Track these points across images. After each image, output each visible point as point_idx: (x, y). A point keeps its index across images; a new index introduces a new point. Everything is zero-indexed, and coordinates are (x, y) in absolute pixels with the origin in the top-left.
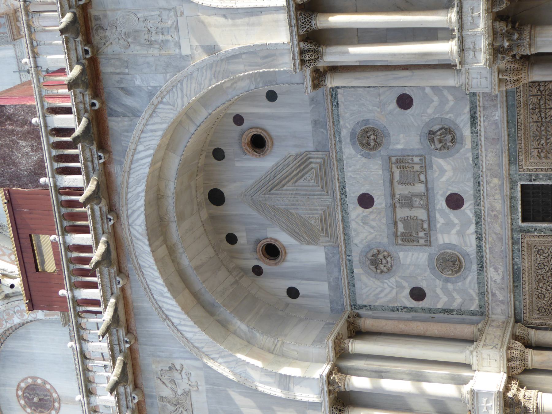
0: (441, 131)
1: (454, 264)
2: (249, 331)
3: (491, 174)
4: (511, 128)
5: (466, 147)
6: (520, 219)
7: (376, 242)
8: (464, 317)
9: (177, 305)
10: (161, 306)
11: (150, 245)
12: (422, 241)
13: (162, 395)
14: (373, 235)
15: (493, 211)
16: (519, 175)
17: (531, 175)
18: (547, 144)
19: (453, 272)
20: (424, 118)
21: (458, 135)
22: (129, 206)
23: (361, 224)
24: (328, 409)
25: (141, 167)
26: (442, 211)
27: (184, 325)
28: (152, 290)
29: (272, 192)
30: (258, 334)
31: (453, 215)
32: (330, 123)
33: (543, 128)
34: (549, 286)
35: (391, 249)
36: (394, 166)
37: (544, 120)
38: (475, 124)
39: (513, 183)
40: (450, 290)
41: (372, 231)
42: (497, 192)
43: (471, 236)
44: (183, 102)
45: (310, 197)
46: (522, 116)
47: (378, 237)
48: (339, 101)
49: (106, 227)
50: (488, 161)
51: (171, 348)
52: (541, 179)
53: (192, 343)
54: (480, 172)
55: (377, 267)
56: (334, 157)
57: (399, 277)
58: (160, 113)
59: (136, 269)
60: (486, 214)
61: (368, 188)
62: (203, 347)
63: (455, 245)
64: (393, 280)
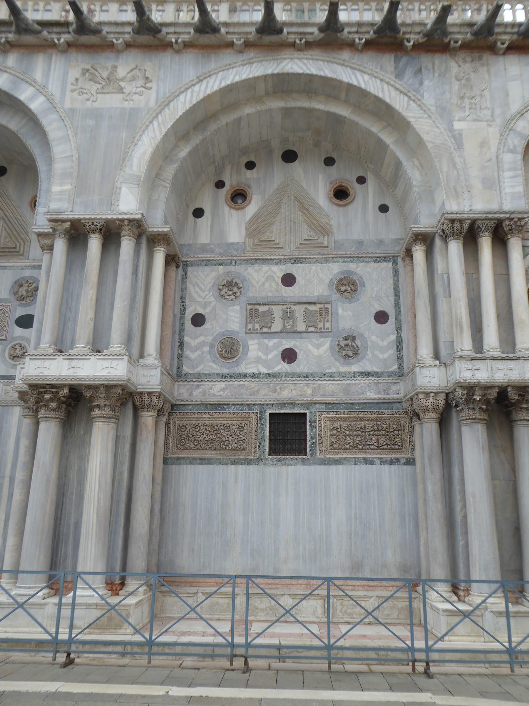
0: (355, 346)
3: (315, 388)
5: (341, 367)
6: (274, 412)
9: (212, 91)
10: (212, 77)
11: (273, 75)
12: (250, 326)
13: (118, 67)
15: (280, 388)
17: (315, 422)
18: (345, 436)
20: (367, 333)
21: (351, 360)
22: (311, 61)
23: (266, 275)
24: (104, 217)
25: (348, 76)
30: (175, 166)
31: (276, 353)
33: (359, 433)
35: (243, 299)
36: (322, 306)
37: (367, 433)
41: (259, 284)
42: (299, 393)
43: (256, 368)
45: (292, 233)
47: (254, 289)
48: (381, 264)
49: (293, 36)
50: (328, 386)
52: (312, 430)
53: (173, 100)
54: (317, 379)
55: (224, 287)
56: (330, 256)
57: (215, 305)
58: (400, 98)
59: (250, 59)
60: (277, 382)
62: (169, 109)
64: (212, 299)
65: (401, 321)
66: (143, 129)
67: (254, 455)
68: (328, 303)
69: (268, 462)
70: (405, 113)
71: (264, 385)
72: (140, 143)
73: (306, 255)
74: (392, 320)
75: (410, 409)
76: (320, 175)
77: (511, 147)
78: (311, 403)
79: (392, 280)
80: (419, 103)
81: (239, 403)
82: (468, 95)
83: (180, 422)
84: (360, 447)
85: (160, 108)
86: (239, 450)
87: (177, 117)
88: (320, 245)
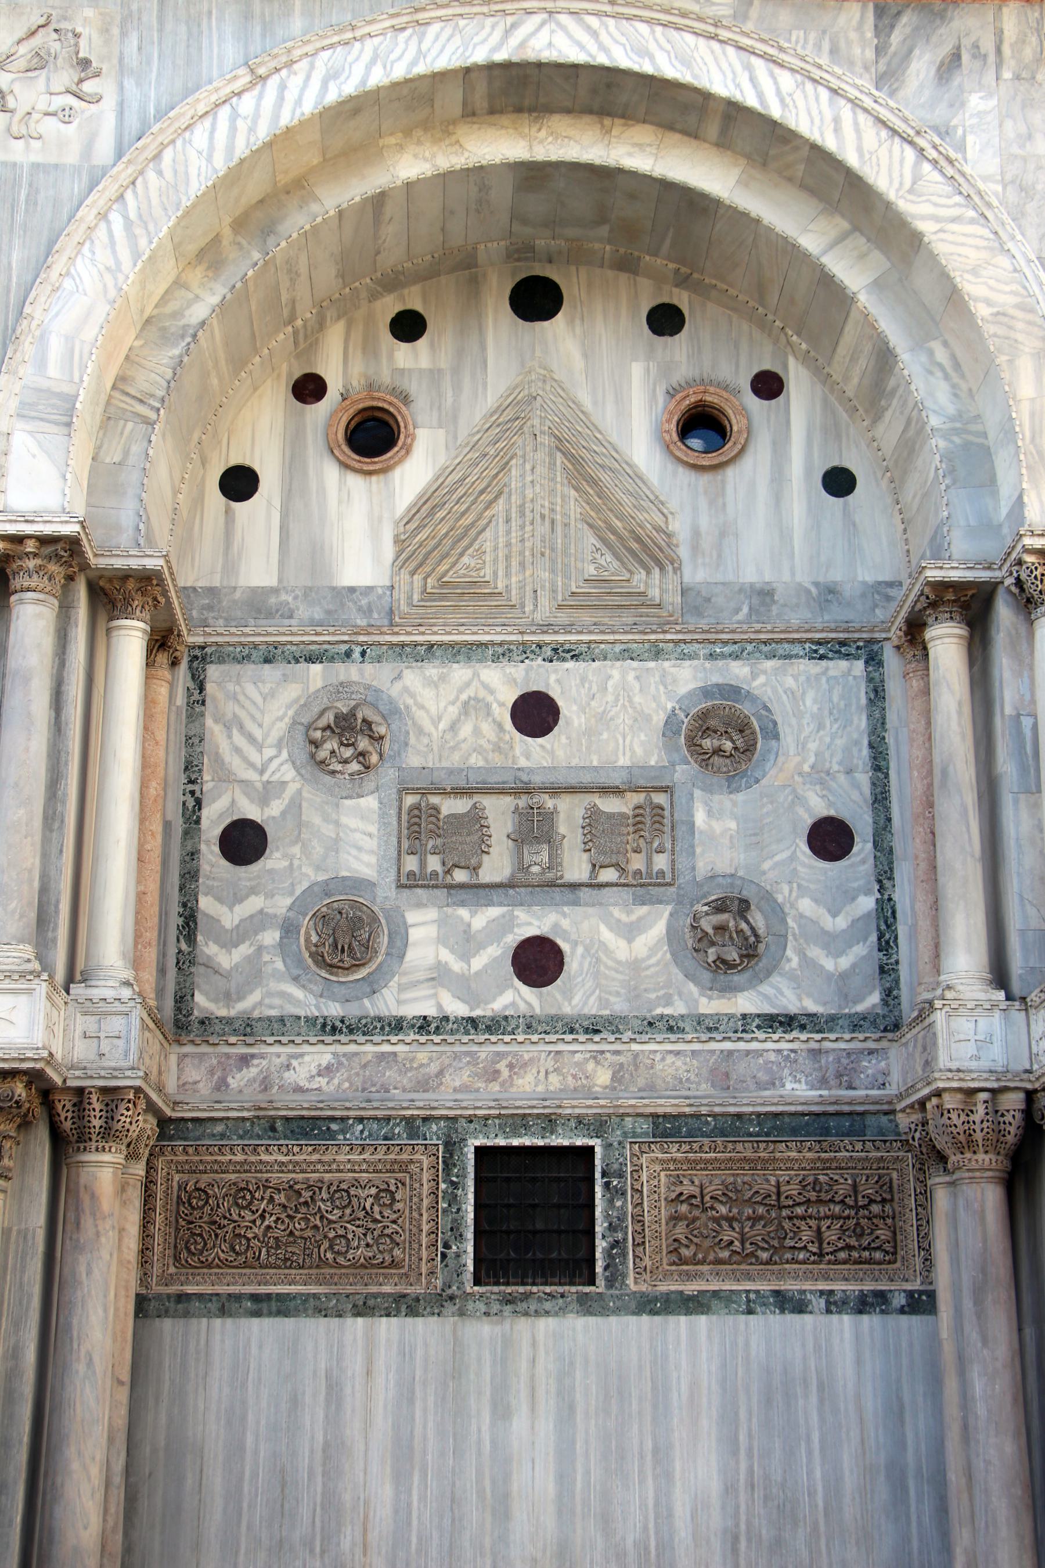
0: (749, 933)
1: (343, 951)
2: (185, 327)
3: (621, 1065)
4: (759, 1124)
5: (704, 1000)
6: (490, 1143)
7: (408, 733)
8: (172, 972)
10: (296, 67)
11: (491, 68)
12: (411, 863)
15: (511, 1066)
16: (620, 1143)
17: (621, 1175)
18: (716, 1220)
19: (316, 946)
20: (786, 889)
21: (736, 978)
22: (611, 22)
23: (464, 697)
25: (730, 76)
26: (507, 924)
27: (233, 129)
28: (347, 48)
29: (559, 455)
32: (768, 632)
33: (761, 1210)
34: (276, 1222)
35: (388, 775)
36: (639, 798)
37: (785, 1213)
38: (771, 1027)
39: (599, 1125)
40: (259, 937)
41: (442, 726)
43: (433, 1002)
44: (924, 218)
46: (793, 1154)
47: (426, 741)
48: (831, 663)
50: (663, 1059)
51: (154, 75)
52: (611, 1202)
54: (628, 1035)
55: (328, 733)
56: (669, 637)
57: (299, 792)
58: (890, 151)
60: (501, 1048)
61: (576, 723)
62: (160, 173)
63: (402, 956)
64: (288, 773)
65: (891, 851)
66: (77, 238)
67: (429, 1283)
68: (664, 789)
69: (470, 1306)
70: (904, 205)
71: (456, 1056)
72: (68, 284)
73: (590, 632)
74: (863, 847)
75: (917, 1135)
76: (634, 364)
78: (609, 1115)
79: (864, 717)
80: (950, 171)
81: (379, 1113)
83: (186, 1177)
84: (764, 1255)
85: (130, 171)
86: (381, 1265)
87: (186, 203)
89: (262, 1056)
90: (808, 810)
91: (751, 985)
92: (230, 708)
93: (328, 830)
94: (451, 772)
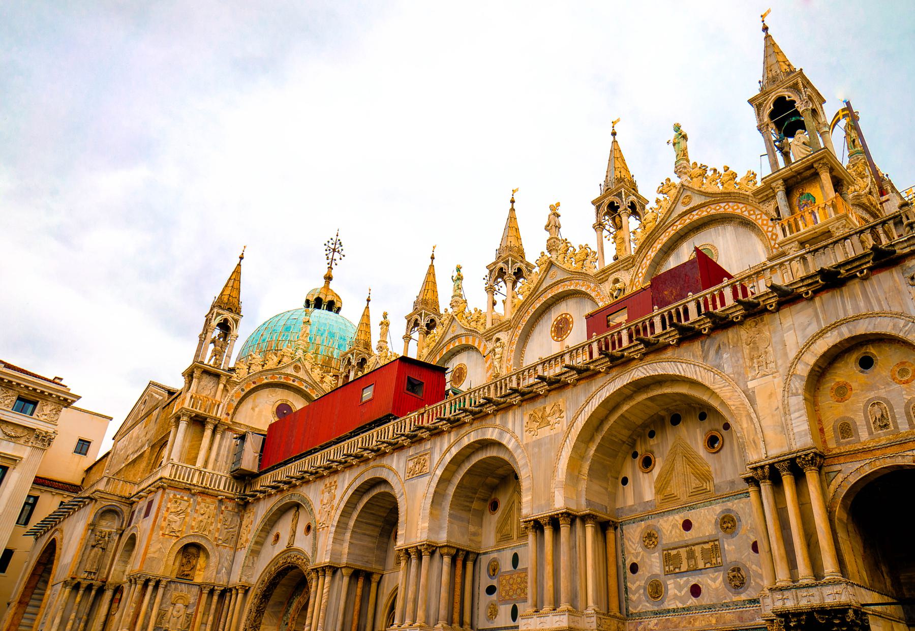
11: (627, 384)
12: (667, 569)
14: (665, 532)
15: (693, 620)
24: (548, 515)
26: (687, 582)
31: (686, 590)
35: (659, 546)
36: (712, 543)
41: (669, 532)
42: (707, 623)
44: (716, 389)
60: (691, 615)
64: (641, 550)
68: (716, 540)
76: (698, 430)
77: (794, 391)
82: (756, 356)
88: (704, 491)
89: (643, 622)
90: (751, 540)
91: (744, 592)
92: (628, 536)
93: (649, 563)
94: (672, 543)
